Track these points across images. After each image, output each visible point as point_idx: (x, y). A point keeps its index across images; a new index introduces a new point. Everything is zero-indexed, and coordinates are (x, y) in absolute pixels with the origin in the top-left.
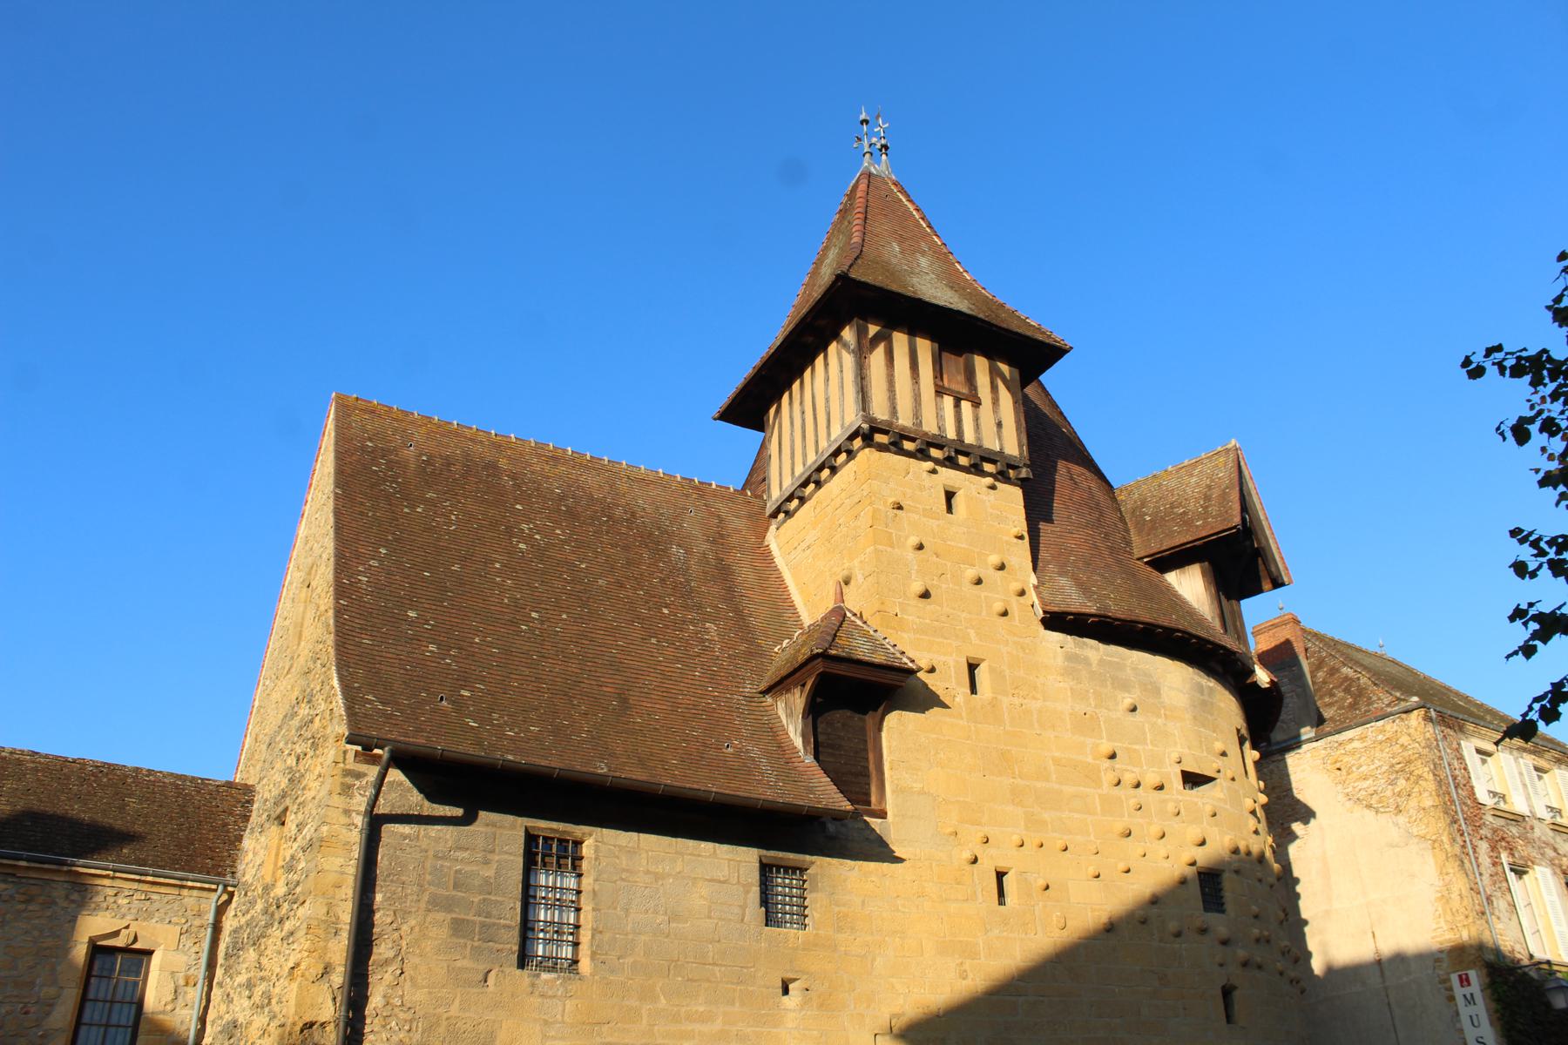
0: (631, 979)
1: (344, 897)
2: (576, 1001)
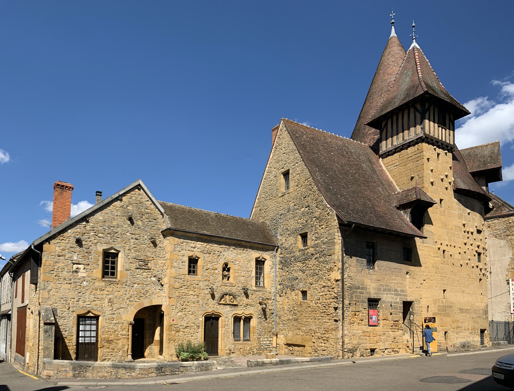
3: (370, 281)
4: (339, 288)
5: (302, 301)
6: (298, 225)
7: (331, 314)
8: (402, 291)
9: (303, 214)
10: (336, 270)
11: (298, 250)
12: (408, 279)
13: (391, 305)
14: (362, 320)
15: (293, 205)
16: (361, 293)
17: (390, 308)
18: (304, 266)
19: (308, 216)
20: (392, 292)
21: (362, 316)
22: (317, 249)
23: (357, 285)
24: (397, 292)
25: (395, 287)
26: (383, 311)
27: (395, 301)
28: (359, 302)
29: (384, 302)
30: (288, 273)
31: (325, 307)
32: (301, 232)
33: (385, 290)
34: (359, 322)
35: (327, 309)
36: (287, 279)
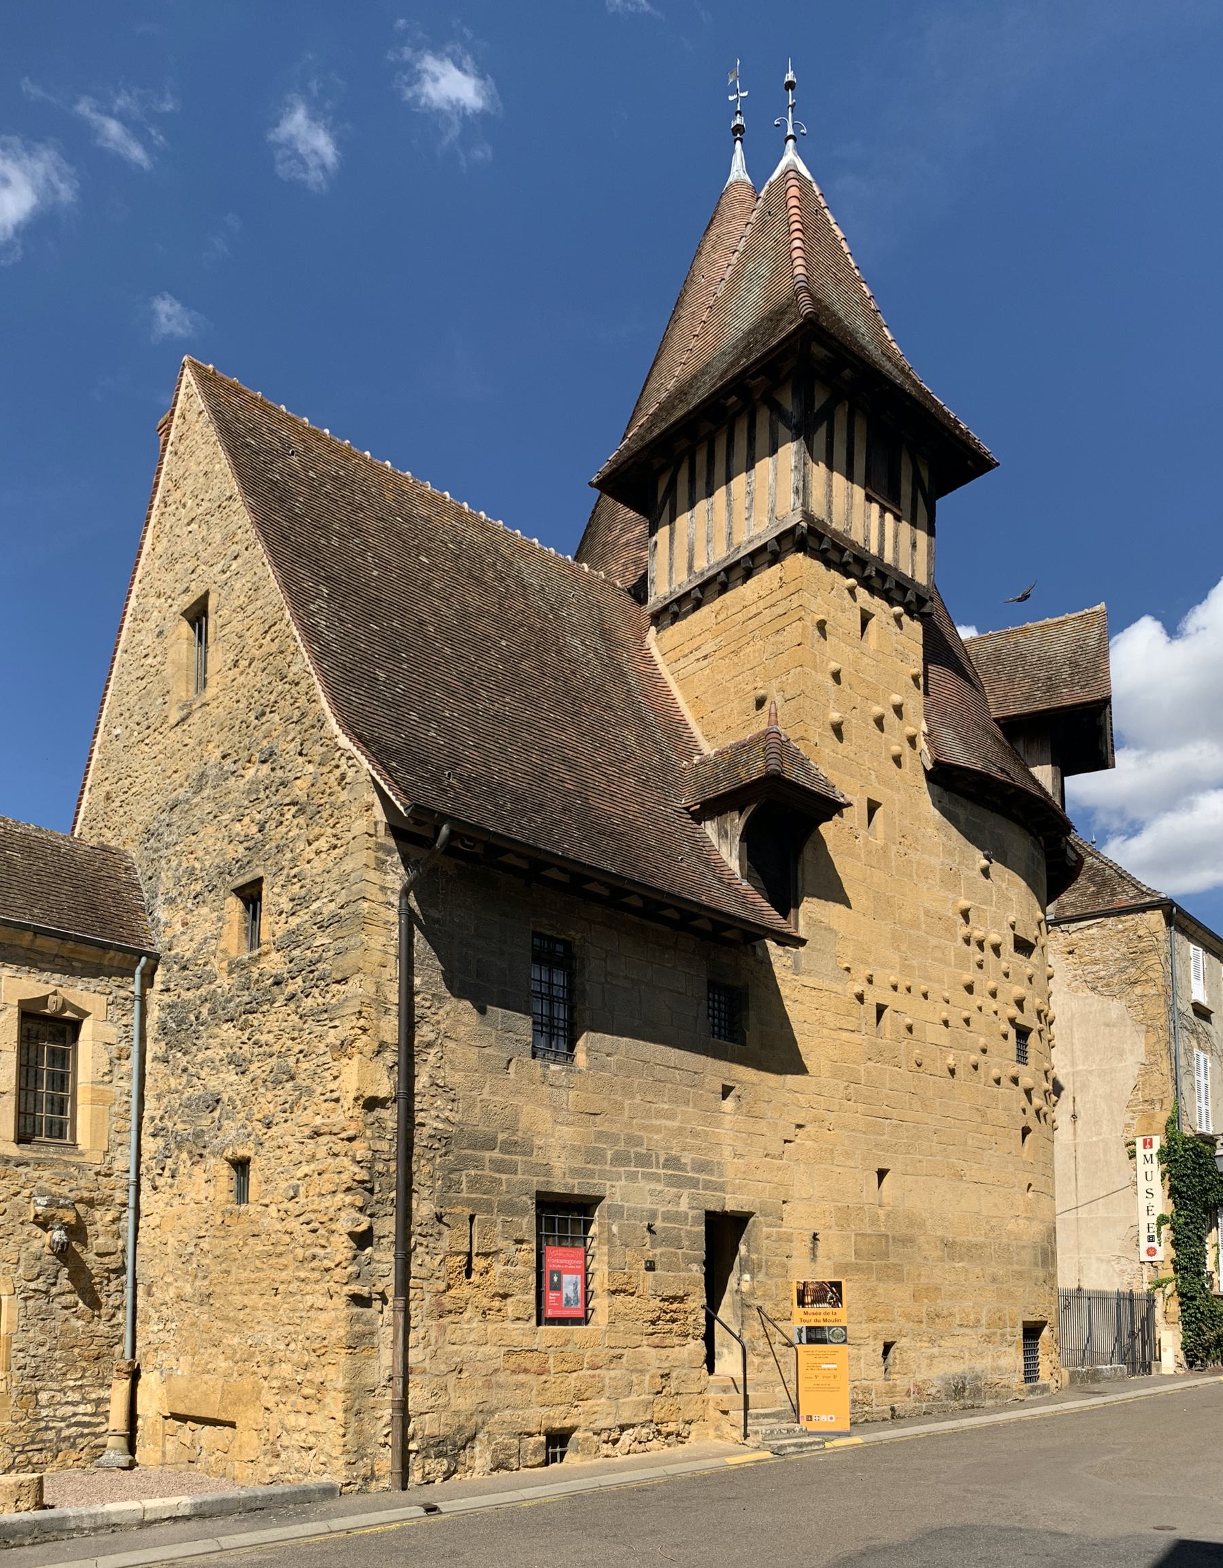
0: (617, 1075)
1: (389, 978)
2: (578, 1092)
3: (547, 1114)
7: (339, 1269)
8: (703, 1167)
12: (729, 1117)
14: (505, 1296)
16: (499, 1167)
17: (648, 1240)
18: (244, 1039)
20: (654, 1170)
21: (504, 1274)
22: (296, 953)
23: (481, 1127)
24: (680, 1170)
25: (672, 1148)
26: (611, 1254)
27: (670, 1207)
28: (489, 1211)
29: (616, 1213)
31: (314, 1231)
32: (240, 881)
33: (621, 1159)
34: (486, 1302)
35: (323, 1242)
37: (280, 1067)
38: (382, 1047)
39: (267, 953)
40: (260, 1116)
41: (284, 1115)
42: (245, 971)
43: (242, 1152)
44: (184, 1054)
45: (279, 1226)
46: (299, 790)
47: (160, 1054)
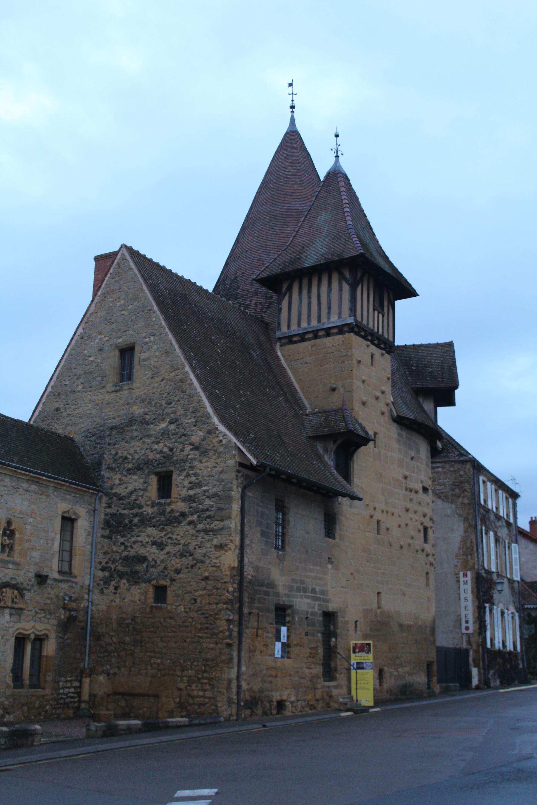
4: (235, 583)
5: (154, 605)
6: (152, 454)
8: (323, 592)
9: (165, 433)
10: (233, 548)
11: (149, 503)
13: (307, 618)
15: (142, 413)
16: (267, 594)
19: (174, 440)
27: (313, 610)
30: (123, 548)
32: (159, 470)
36: (120, 559)
37: (184, 550)
38: (236, 546)
39: (177, 502)
40: (173, 569)
41: (188, 570)
42: (162, 508)
43: (162, 582)
44: (122, 537)
45: (185, 615)
46: (195, 439)
47: (105, 534)
